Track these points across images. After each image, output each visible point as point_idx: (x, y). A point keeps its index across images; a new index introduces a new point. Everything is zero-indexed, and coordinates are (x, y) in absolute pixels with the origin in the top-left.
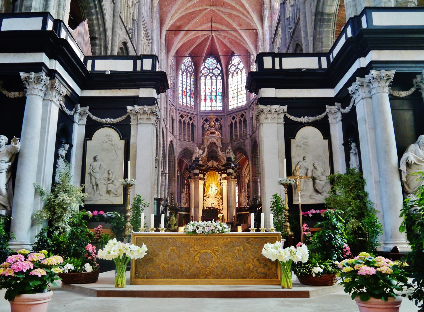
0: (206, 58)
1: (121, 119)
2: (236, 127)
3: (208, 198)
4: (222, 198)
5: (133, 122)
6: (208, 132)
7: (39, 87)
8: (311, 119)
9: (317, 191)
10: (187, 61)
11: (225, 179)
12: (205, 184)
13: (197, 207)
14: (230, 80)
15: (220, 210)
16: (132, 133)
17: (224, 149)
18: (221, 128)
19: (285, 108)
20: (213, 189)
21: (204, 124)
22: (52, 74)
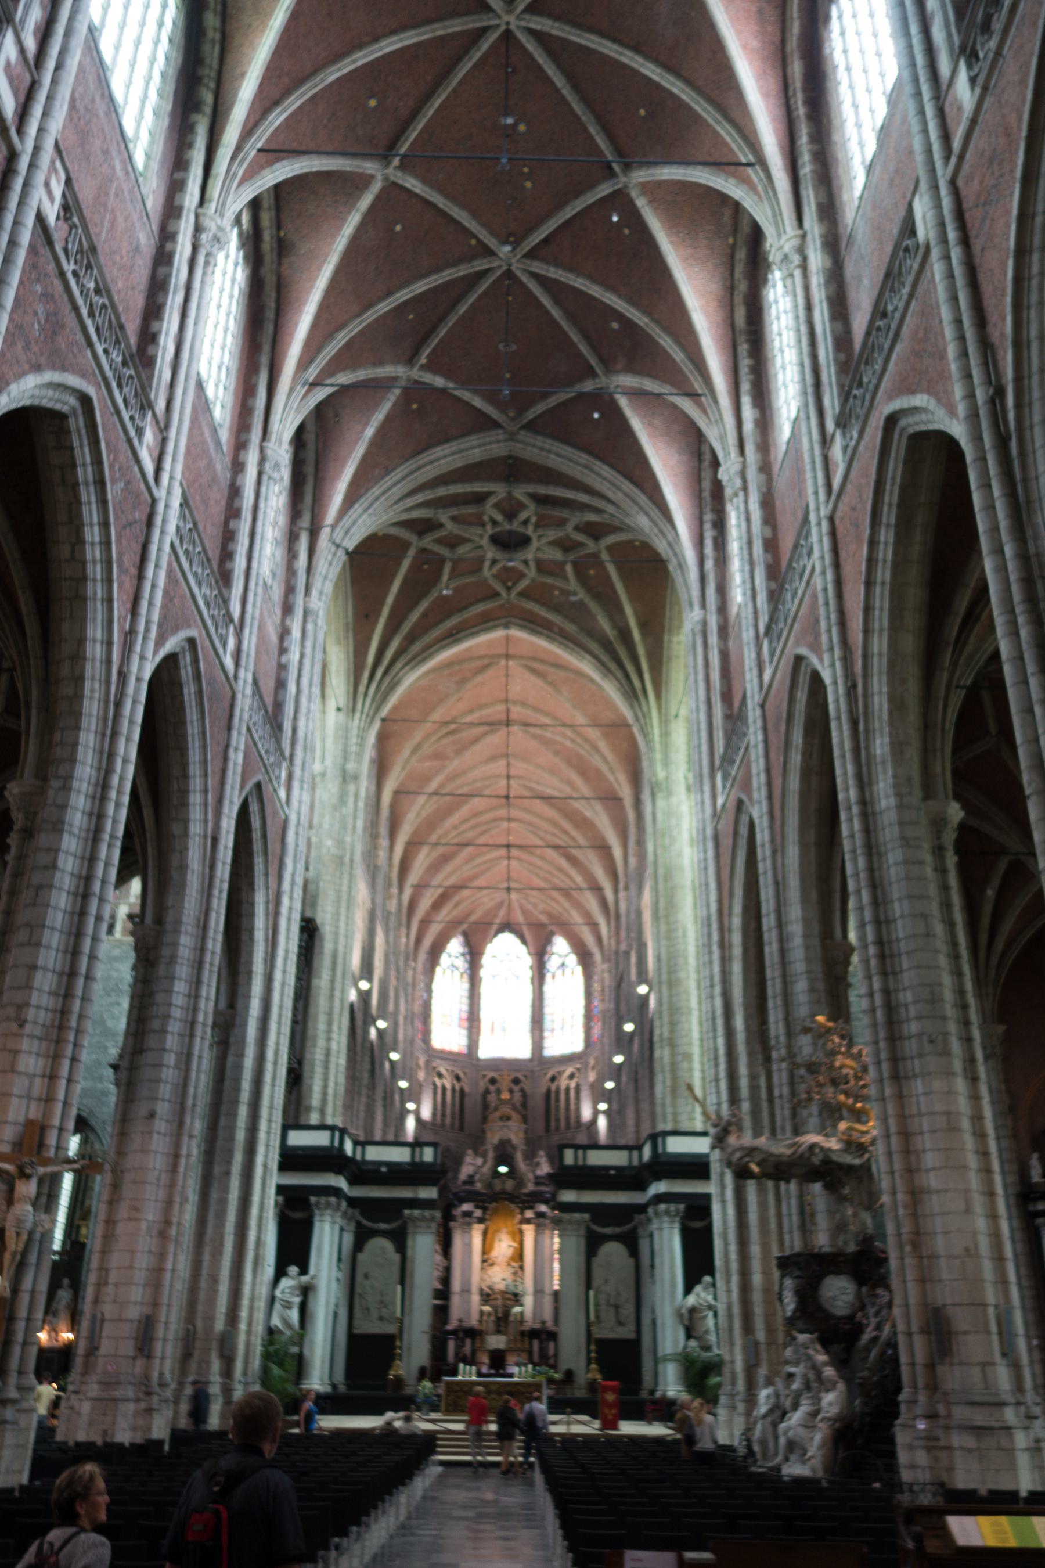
0: (496, 935)
1: (394, 1225)
2: (557, 1100)
3: (492, 1265)
4: (522, 1268)
5: (410, 1229)
6: (498, 1114)
7: (329, 1212)
8: (617, 1230)
9: (620, 1323)
10: (455, 946)
11: (528, 1221)
12: (485, 1234)
13: (466, 1290)
14: (548, 988)
15: (516, 1295)
16: (410, 1243)
17: (530, 1156)
18: (524, 1105)
19: (586, 1216)
20: (503, 1247)
21: (487, 1092)
22: (337, 1192)
